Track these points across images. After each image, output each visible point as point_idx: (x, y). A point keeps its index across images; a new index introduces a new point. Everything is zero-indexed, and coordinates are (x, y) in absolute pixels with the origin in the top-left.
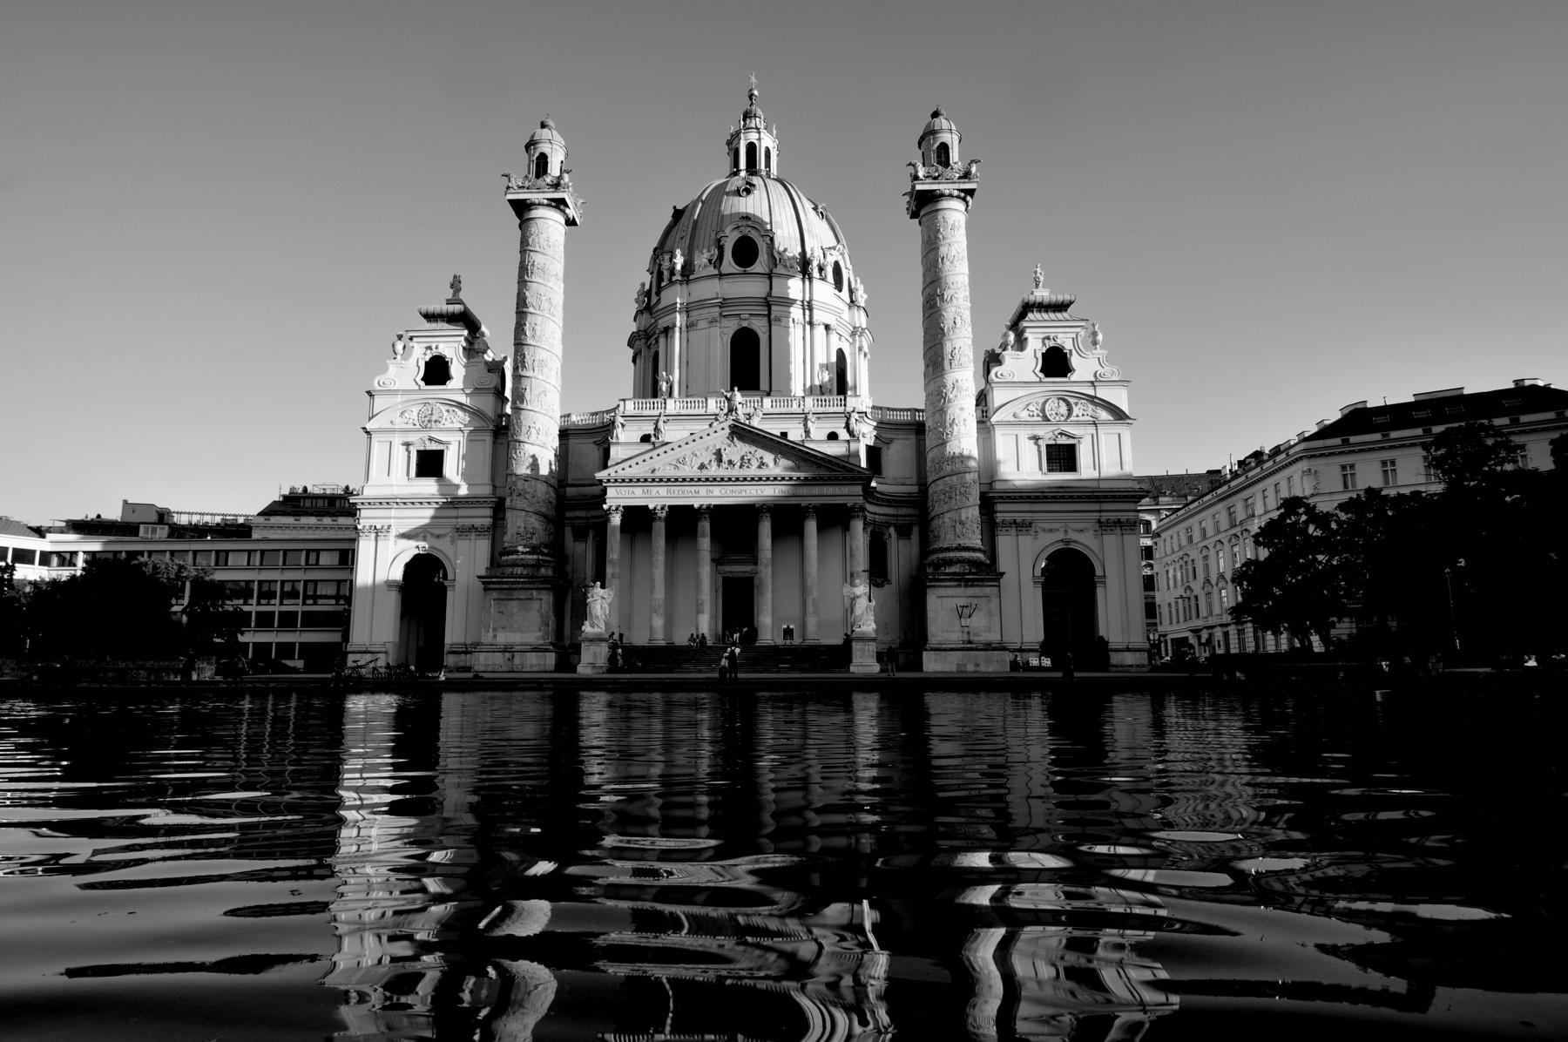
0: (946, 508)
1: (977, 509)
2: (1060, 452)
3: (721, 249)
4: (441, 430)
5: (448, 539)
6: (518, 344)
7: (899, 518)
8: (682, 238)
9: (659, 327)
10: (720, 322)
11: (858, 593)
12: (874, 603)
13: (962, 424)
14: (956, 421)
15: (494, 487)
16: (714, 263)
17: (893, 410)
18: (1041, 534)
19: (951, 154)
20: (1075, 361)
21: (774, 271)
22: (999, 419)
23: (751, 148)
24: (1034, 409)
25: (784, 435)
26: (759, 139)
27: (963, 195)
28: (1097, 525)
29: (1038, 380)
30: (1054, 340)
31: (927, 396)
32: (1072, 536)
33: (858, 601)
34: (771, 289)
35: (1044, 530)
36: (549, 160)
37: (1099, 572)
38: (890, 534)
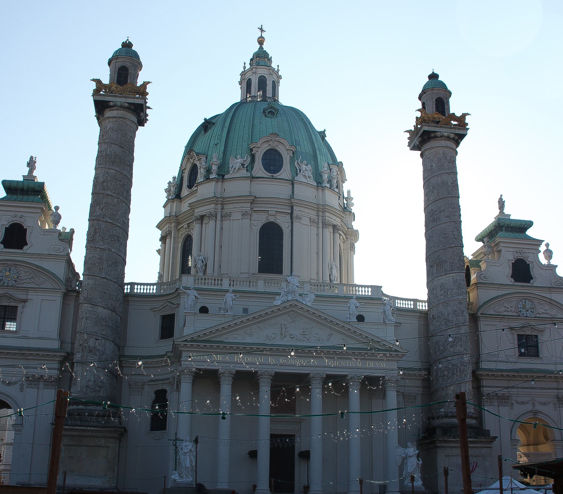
3: (253, 157)
4: (18, 288)
5: (18, 386)
6: (95, 220)
8: (218, 144)
9: (195, 215)
10: (251, 216)
15: (62, 343)
16: (247, 167)
19: (446, 106)
20: (534, 272)
23: (262, 82)
27: (456, 138)
28: (556, 400)
30: (521, 254)
32: (538, 407)
34: (293, 193)
35: (518, 402)
36: (130, 71)
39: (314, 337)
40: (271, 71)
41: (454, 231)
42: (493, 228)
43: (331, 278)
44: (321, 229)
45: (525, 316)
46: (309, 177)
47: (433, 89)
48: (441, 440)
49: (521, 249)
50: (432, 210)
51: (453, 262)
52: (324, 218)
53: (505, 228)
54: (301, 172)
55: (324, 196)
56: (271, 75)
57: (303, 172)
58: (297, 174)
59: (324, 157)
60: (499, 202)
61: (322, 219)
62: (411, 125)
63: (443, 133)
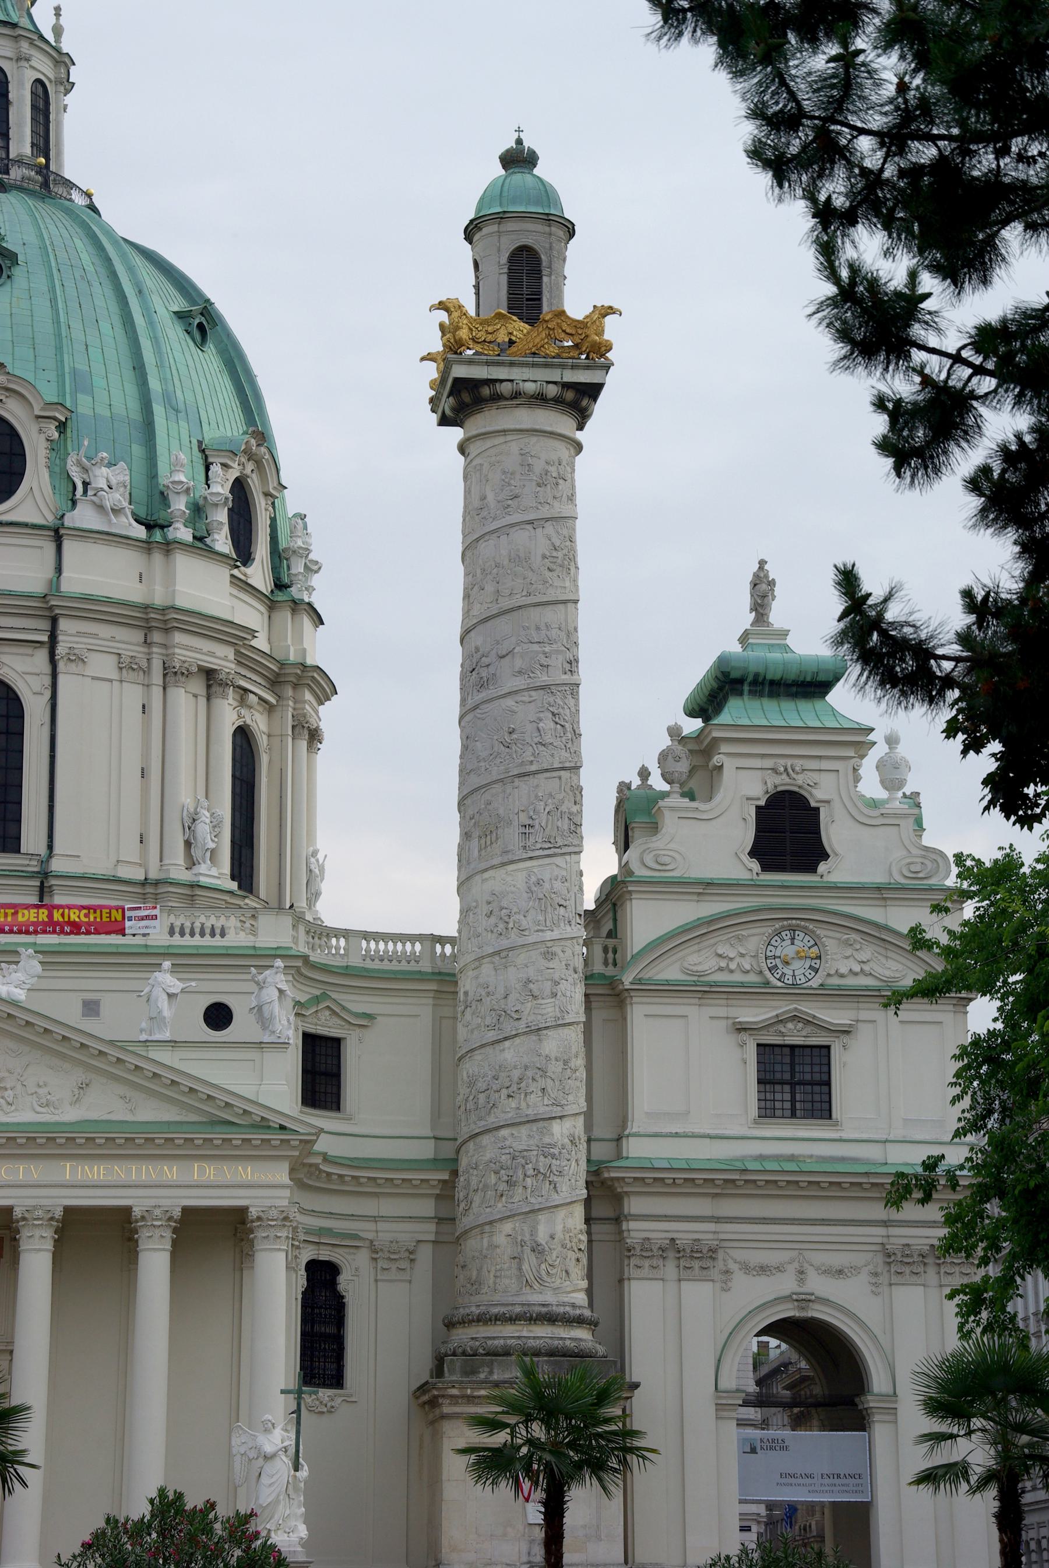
0: (501, 1208)
1: (579, 1211)
2: (792, 1065)
7: (382, 1226)
11: (269, 1449)
12: (304, 1473)
13: (548, 992)
14: (531, 986)
17: (377, 936)
18: (739, 1279)
19: (545, 279)
21: (68, 522)
22: (646, 975)
24: (731, 955)
25: (91, 1008)
26: (19, 59)
27: (570, 395)
28: (880, 1259)
29: (744, 875)
30: (788, 774)
31: (466, 912)
32: (818, 1285)
33: (269, 1468)
34: (59, 569)
35: (746, 1268)
37: (878, 1381)
38: (357, 1269)
39: (32, 1094)
40: (25, 45)
41: (541, 720)
42: (715, 685)
43: (193, 854)
44: (157, 692)
45: (790, 982)
46: (117, 511)
47: (502, 218)
48: (452, 1396)
49: (789, 762)
50: (477, 650)
51: (531, 822)
52: (170, 651)
53: (750, 684)
54: (90, 493)
55: (170, 578)
56: (24, 63)
57: (95, 495)
58: (74, 503)
59: (183, 424)
60: (754, 585)
61: (163, 655)
62: (436, 345)
63: (521, 384)
